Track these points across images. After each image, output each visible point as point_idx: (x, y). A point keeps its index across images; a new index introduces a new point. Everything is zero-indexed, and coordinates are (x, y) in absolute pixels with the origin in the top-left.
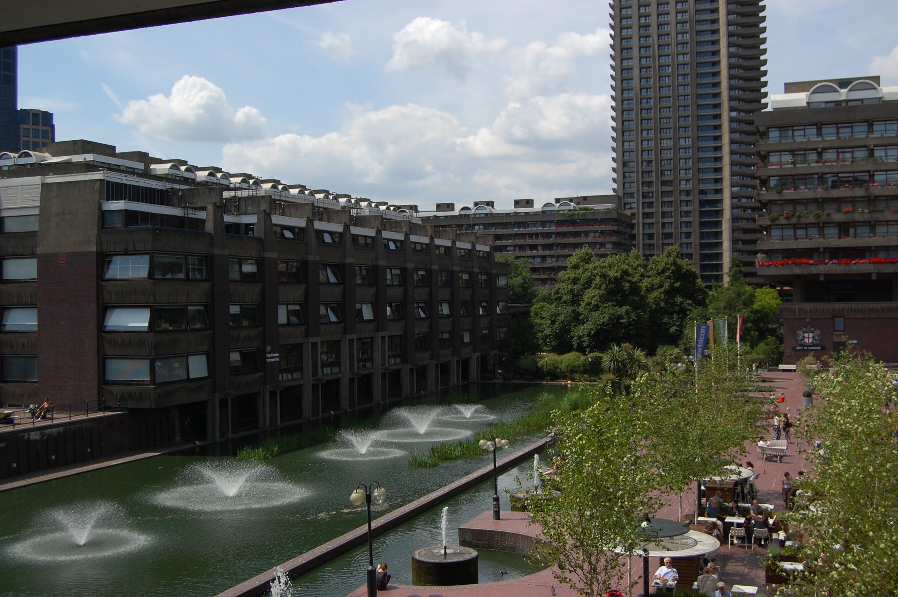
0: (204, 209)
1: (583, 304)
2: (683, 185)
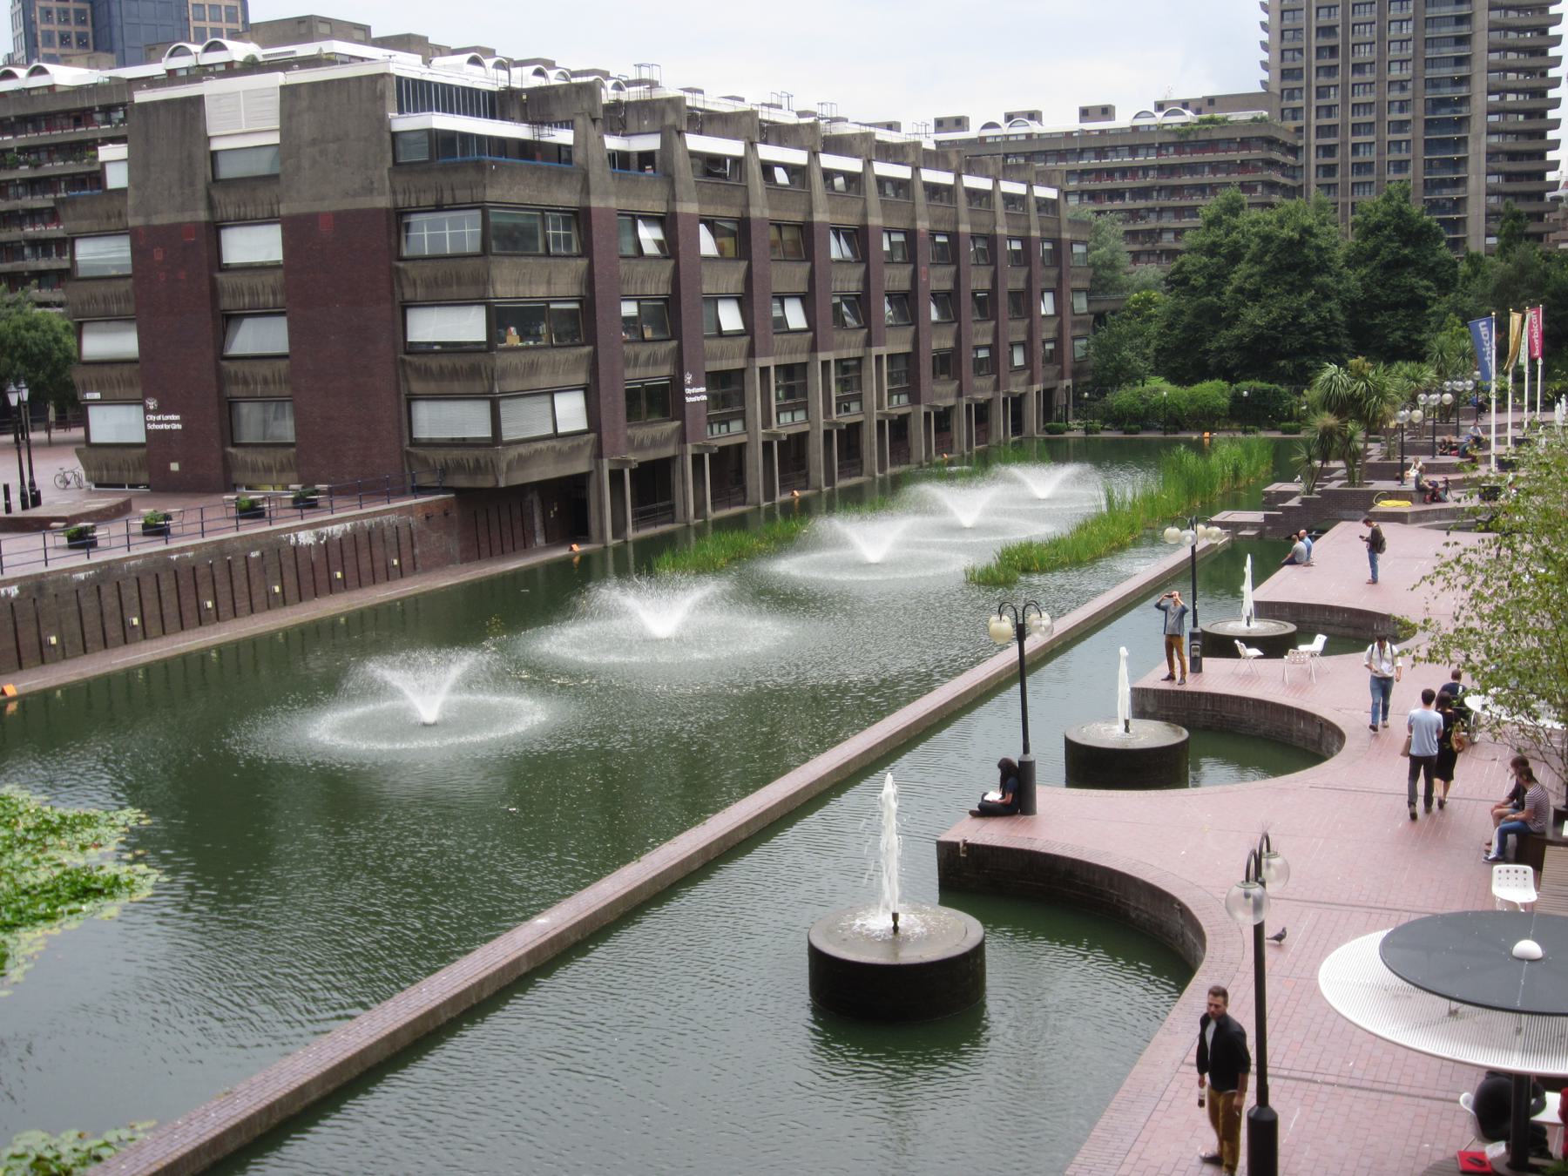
0: (567, 124)
1: (1229, 289)
2: (1395, 73)
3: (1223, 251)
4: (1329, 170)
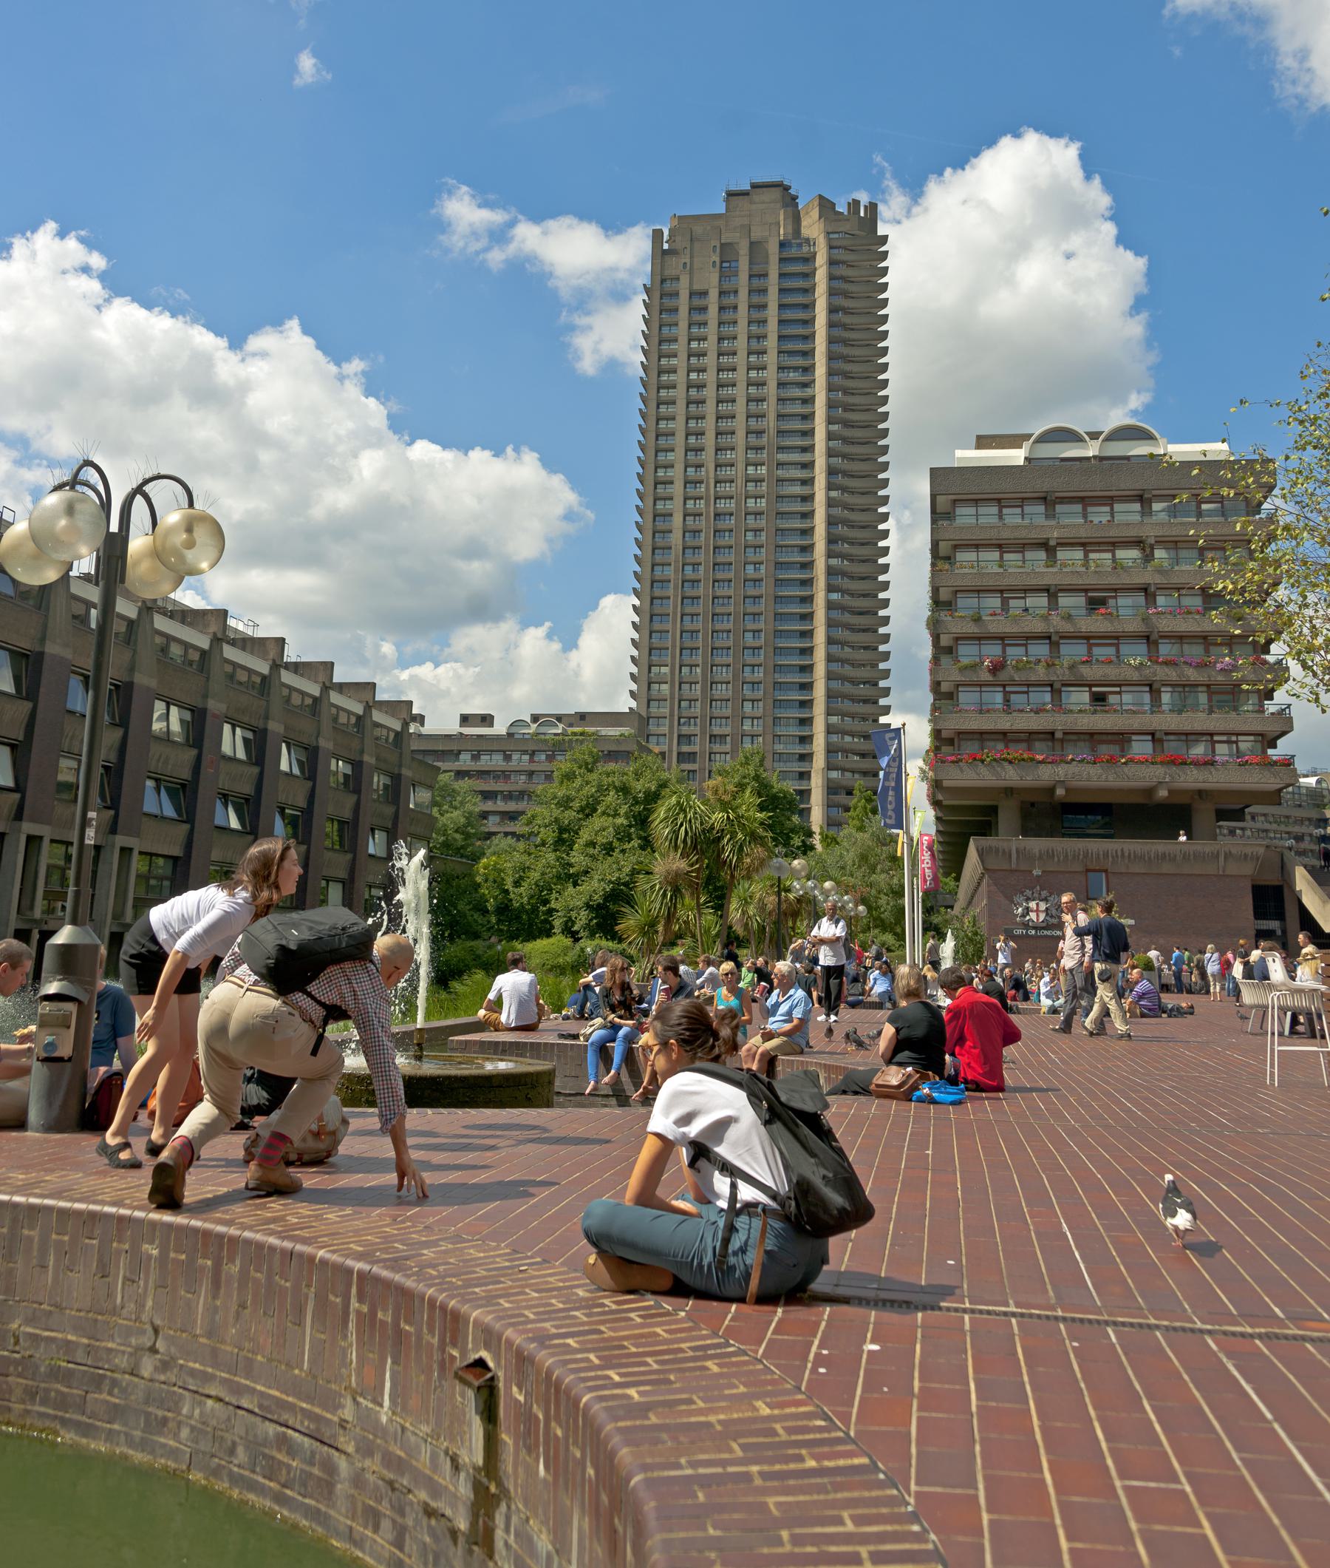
3: (576, 805)
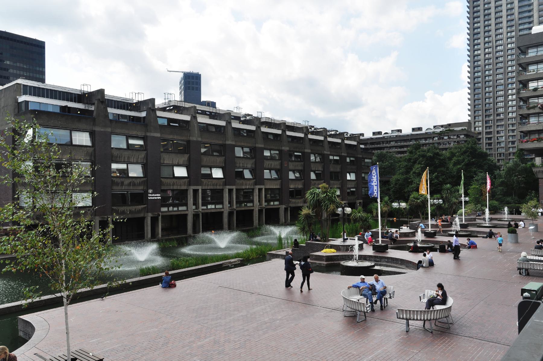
3: (412, 161)
4: (490, 144)
